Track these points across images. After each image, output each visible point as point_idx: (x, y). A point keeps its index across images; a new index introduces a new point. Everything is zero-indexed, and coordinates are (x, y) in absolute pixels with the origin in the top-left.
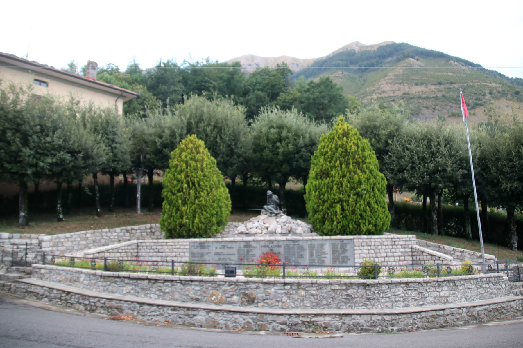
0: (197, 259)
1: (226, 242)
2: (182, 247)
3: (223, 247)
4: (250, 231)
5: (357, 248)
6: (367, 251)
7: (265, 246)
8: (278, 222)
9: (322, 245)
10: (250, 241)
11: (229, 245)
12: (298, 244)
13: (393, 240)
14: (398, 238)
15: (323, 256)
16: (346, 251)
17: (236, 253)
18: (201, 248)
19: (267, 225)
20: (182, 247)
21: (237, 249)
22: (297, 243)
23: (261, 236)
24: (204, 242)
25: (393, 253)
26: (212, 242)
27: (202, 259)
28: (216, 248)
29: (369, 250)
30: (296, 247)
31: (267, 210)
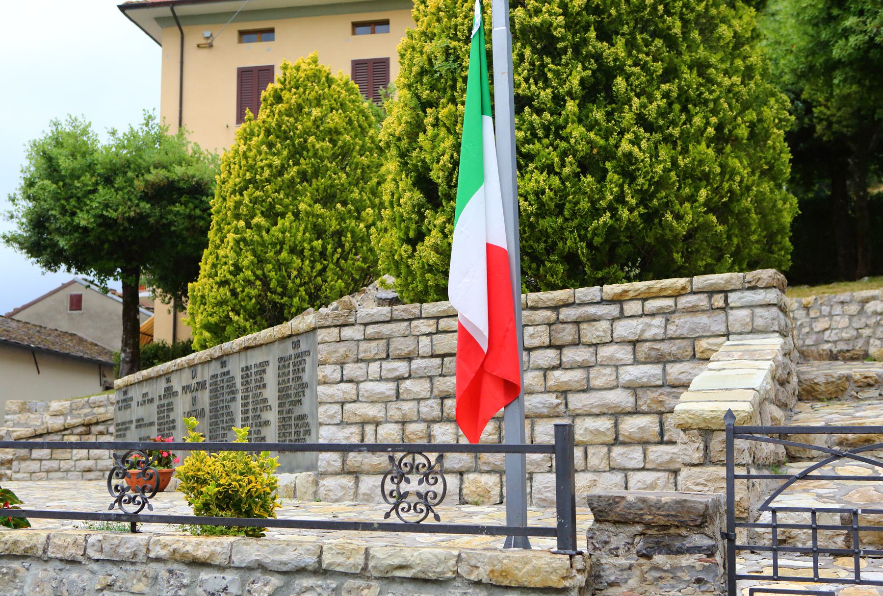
5: (330, 372)
6: (388, 388)
13: (565, 313)
14: (602, 302)
25: (564, 393)
29: (399, 379)
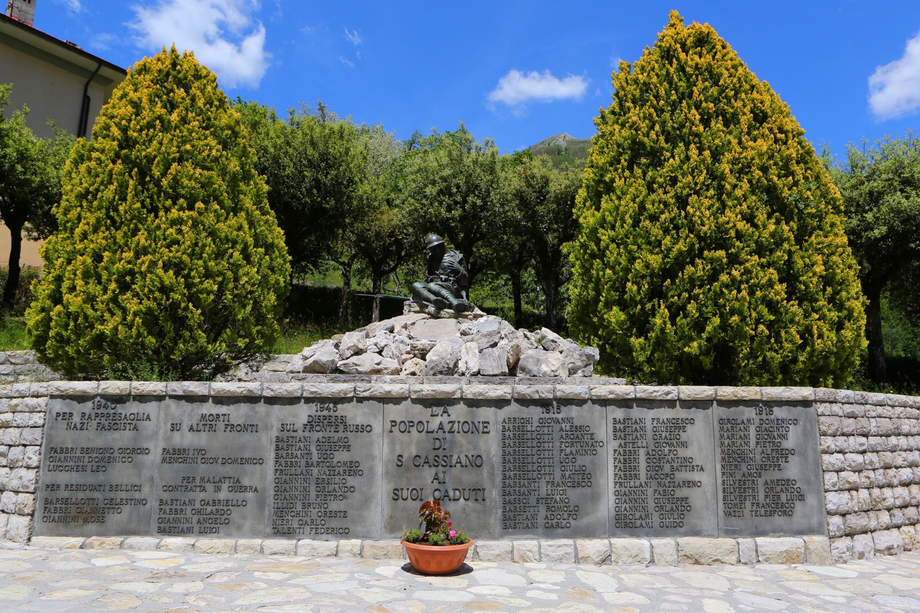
0: (73, 478)
1: (221, 399)
2: (19, 418)
3: (208, 424)
4: (354, 359)
7: (408, 426)
8: (464, 334)
9: (678, 426)
10: (338, 400)
11: (238, 413)
12: (569, 420)
15: (681, 476)
16: (785, 454)
17: (270, 456)
18: (101, 427)
19: (423, 342)
20: (19, 418)
21: (275, 433)
22: (560, 416)
23: (393, 381)
24: (120, 399)
26: (160, 398)
27: (100, 477)
28: (175, 427)
30: (556, 435)
31: (426, 293)
